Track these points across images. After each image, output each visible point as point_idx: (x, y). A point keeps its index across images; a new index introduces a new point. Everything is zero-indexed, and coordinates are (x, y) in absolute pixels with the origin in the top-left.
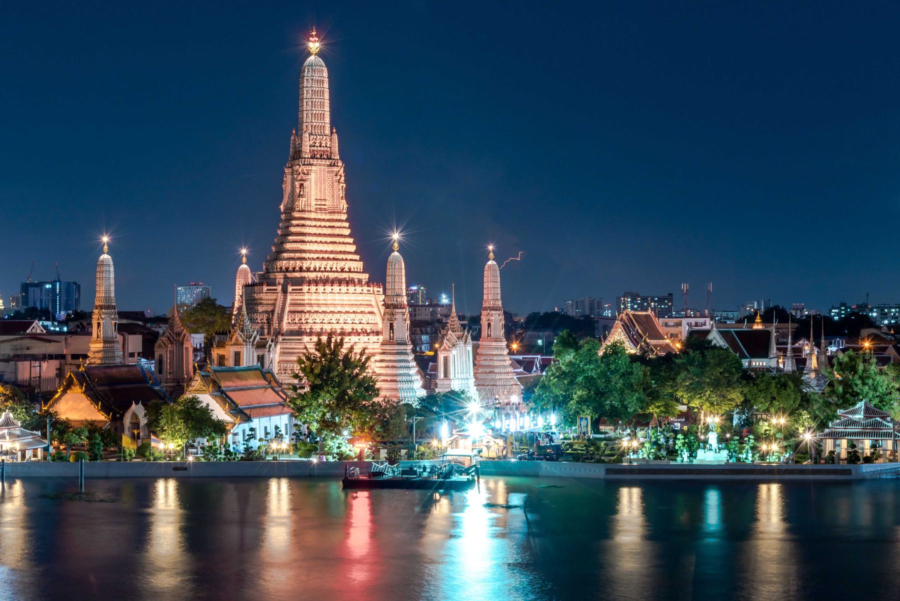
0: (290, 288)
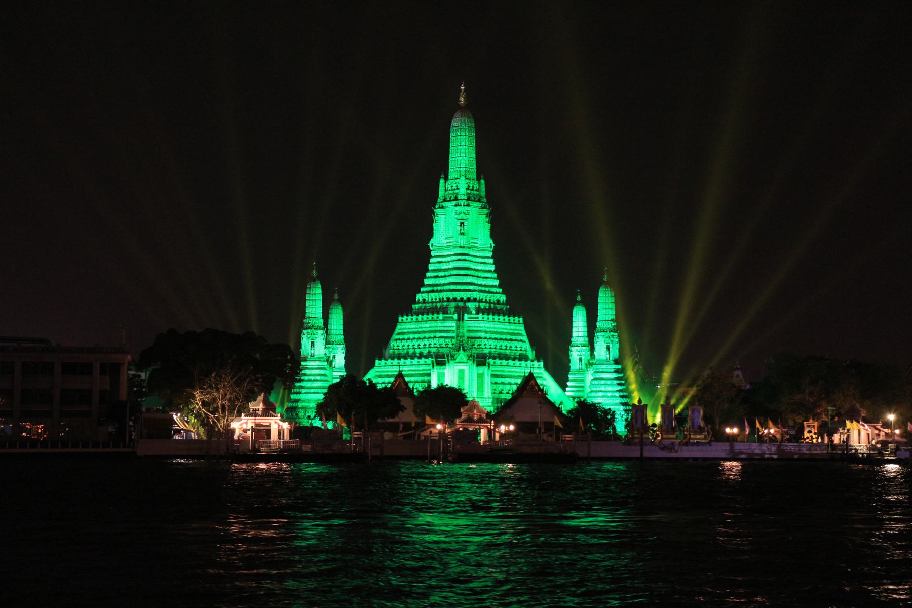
0: (466, 316)
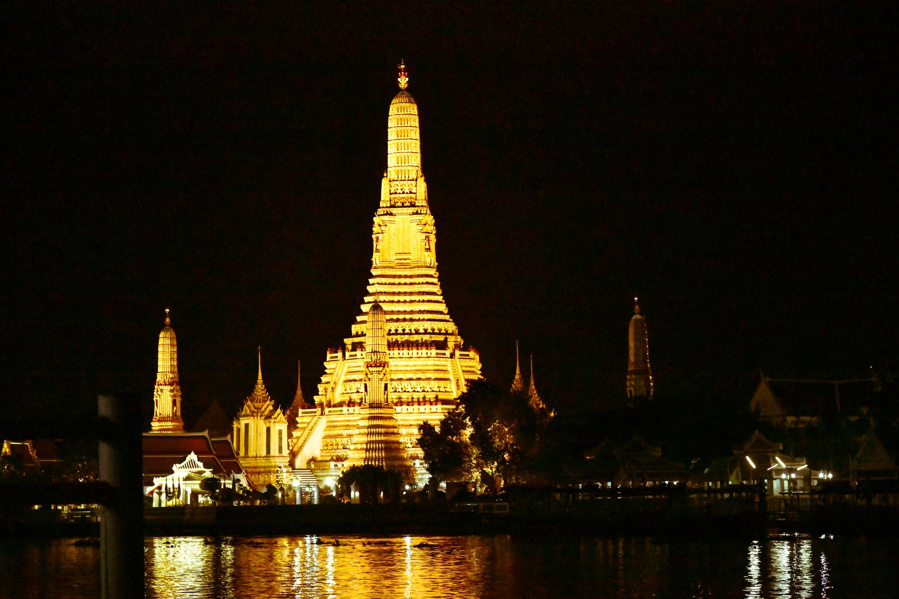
0: (458, 353)
